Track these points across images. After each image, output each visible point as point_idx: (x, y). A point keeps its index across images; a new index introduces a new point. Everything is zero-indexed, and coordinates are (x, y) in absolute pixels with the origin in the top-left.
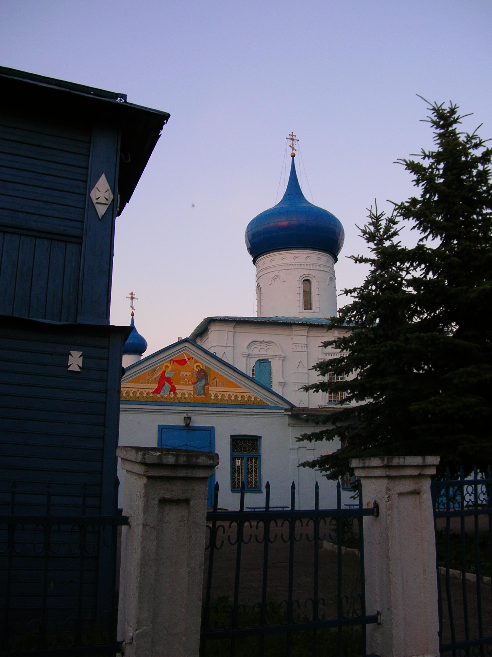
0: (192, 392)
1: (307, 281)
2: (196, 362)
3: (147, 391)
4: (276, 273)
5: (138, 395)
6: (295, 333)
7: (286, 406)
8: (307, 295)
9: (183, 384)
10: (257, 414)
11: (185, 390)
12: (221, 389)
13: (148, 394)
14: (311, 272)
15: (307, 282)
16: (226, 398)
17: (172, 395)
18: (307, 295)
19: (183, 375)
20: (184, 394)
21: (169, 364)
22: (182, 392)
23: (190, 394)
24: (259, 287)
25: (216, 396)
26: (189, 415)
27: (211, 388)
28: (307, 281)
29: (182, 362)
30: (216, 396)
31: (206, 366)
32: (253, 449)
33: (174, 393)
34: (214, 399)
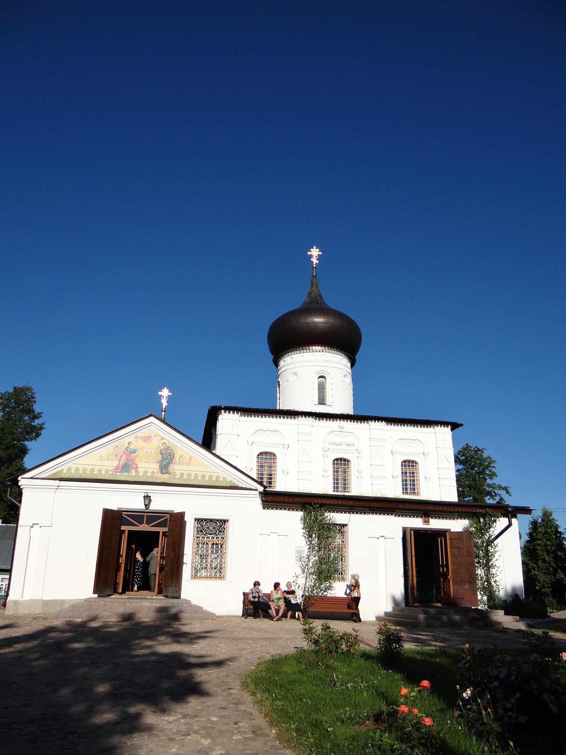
3: (106, 468)
5: (96, 473)
7: (261, 489)
11: (148, 467)
13: (107, 471)
14: (323, 369)
16: (193, 478)
19: (147, 452)
20: (146, 472)
22: (144, 470)
25: (182, 474)
26: (149, 495)
29: (147, 439)
30: (182, 474)
31: (172, 444)
32: (220, 531)
34: (179, 478)
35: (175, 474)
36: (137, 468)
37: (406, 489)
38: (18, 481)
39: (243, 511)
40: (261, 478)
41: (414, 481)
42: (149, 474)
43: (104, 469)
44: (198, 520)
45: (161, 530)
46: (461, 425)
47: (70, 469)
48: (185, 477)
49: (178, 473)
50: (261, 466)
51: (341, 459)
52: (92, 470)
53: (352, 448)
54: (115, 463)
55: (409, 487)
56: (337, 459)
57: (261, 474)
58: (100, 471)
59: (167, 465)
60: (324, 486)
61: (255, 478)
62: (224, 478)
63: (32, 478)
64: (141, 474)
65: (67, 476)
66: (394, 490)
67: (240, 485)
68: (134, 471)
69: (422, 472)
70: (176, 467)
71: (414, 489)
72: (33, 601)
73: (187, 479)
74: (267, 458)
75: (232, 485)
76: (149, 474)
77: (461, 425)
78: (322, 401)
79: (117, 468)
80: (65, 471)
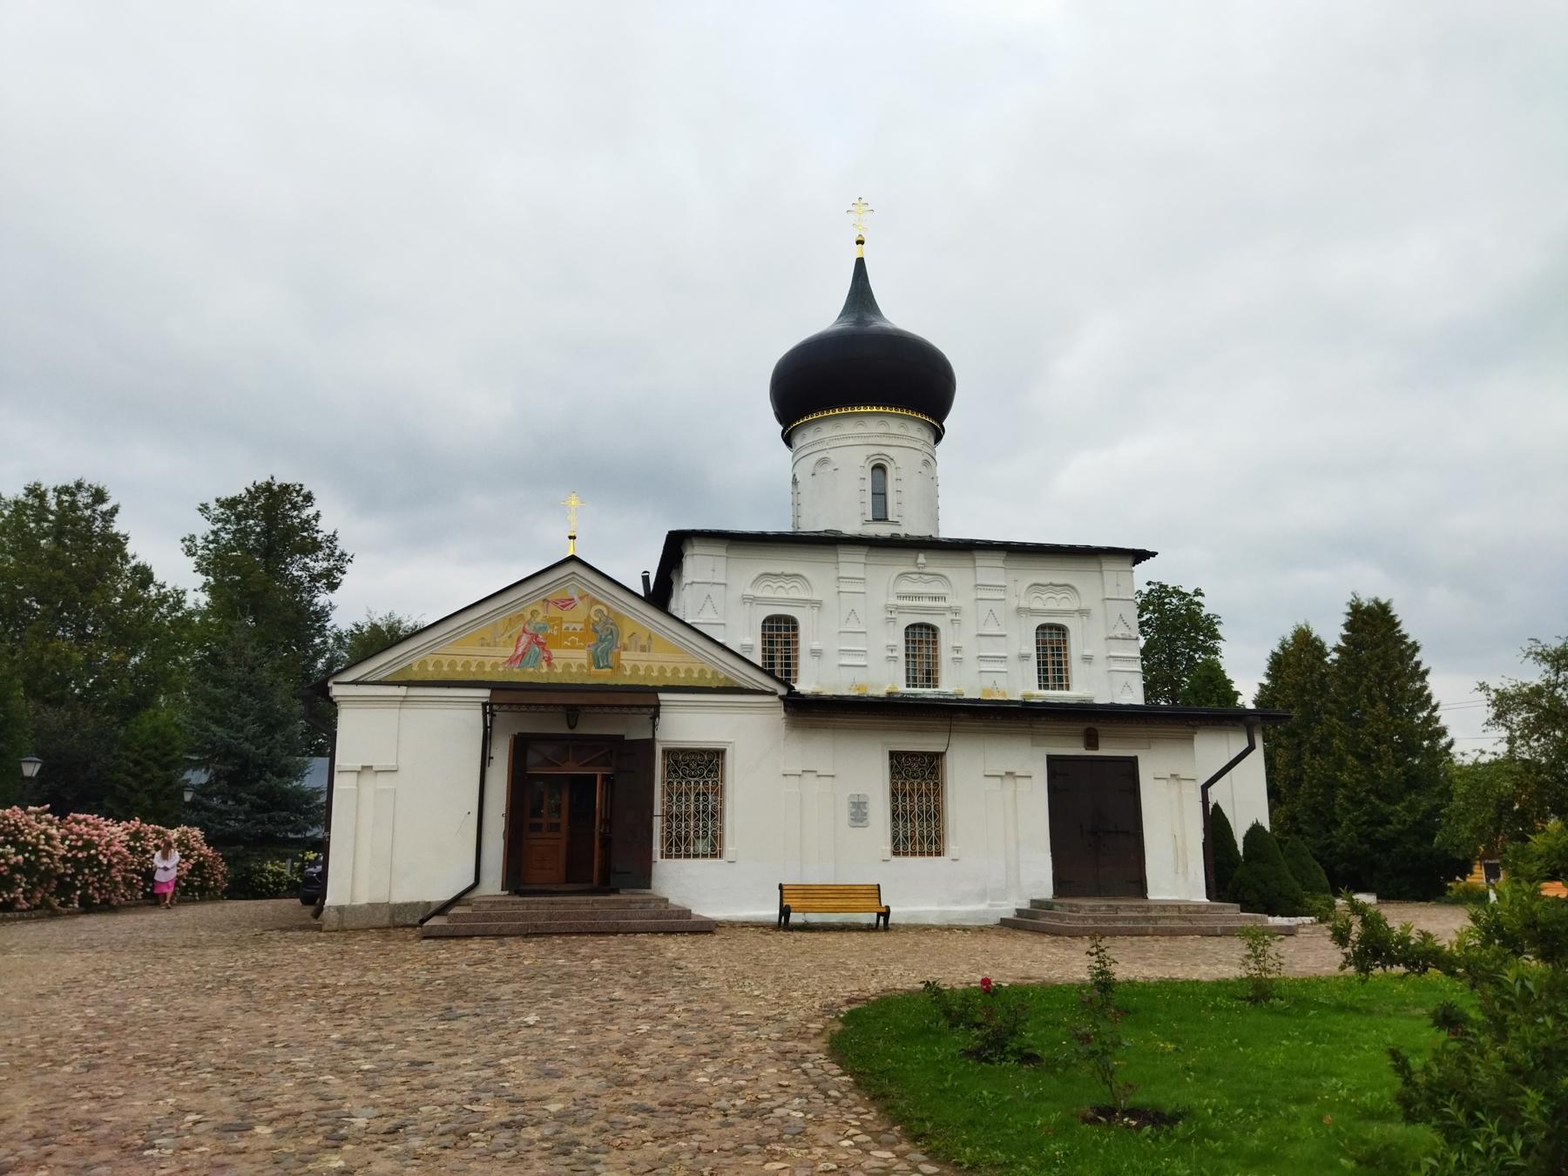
0: (585, 662)
1: (879, 469)
2: (598, 602)
3: (493, 660)
4: (823, 454)
6: (842, 558)
7: (782, 691)
8: (880, 495)
9: (567, 647)
10: (733, 706)
12: (644, 656)
13: (495, 666)
15: (879, 472)
16: (655, 674)
17: (545, 669)
18: (880, 495)
20: (568, 666)
21: (540, 610)
22: (563, 662)
23: (581, 666)
24: (795, 482)
25: (635, 669)
27: (624, 655)
28: (879, 469)
29: (566, 604)
30: (635, 669)
33: (549, 665)
35: (620, 667)
36: (549, 660)
37: (1046, 679)
38: (328, 690)
39: (744, 734)
40: (772, 665)
41: (1060, 663)
42: (574, 670)
43: (489, 662)
44: (668, 753)
45: (599, 773)
46: (1154, 554)
47: (423, 663)
48: (642, 673)
49: (628, 665)
50: (768, 642)
51: (921, 625)
52: (466, 665)
53: (941, 604)
54: (510, 651)
55: (1050, 675)
56: (913, 626)
57: (769, 656)
58: (481, 665)
59: (606, 653)
60: (886, 676)
61: (759, 663)
62: (714, 673)
63: (355, 683)
64: (559, 670)
65: (419, 678)
66: (1022, 685)
67: (745, 685)
68: (544, 664)
69: (1076, 648)
70: (624, 655)
71: (1060, 679)
72: (374, 907)
73: (644, 677)
74: (780, 631)
75: (728, 684)
76: (574, 670)
77: (1154, 554)
78: (881, 516)
79: (511, 661)
80: (415, 668)
